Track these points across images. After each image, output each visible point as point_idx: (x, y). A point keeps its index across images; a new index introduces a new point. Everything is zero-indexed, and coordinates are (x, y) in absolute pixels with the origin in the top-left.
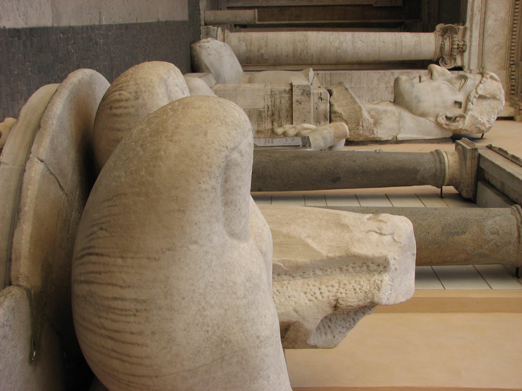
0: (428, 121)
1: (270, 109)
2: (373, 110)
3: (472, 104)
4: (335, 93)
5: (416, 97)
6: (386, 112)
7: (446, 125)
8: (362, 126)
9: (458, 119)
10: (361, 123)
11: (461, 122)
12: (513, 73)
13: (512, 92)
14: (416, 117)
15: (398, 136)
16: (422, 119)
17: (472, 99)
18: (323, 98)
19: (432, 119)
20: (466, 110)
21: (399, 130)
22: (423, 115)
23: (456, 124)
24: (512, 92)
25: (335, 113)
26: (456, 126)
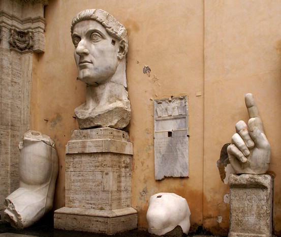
1: (117, 168)
5: (107, 69)
6: (111, 91)
9: (122, 46)
15: (126, 87)
19: (119, 62)
20: (118, 39)
23: (126, 47)
25: (116, 125)
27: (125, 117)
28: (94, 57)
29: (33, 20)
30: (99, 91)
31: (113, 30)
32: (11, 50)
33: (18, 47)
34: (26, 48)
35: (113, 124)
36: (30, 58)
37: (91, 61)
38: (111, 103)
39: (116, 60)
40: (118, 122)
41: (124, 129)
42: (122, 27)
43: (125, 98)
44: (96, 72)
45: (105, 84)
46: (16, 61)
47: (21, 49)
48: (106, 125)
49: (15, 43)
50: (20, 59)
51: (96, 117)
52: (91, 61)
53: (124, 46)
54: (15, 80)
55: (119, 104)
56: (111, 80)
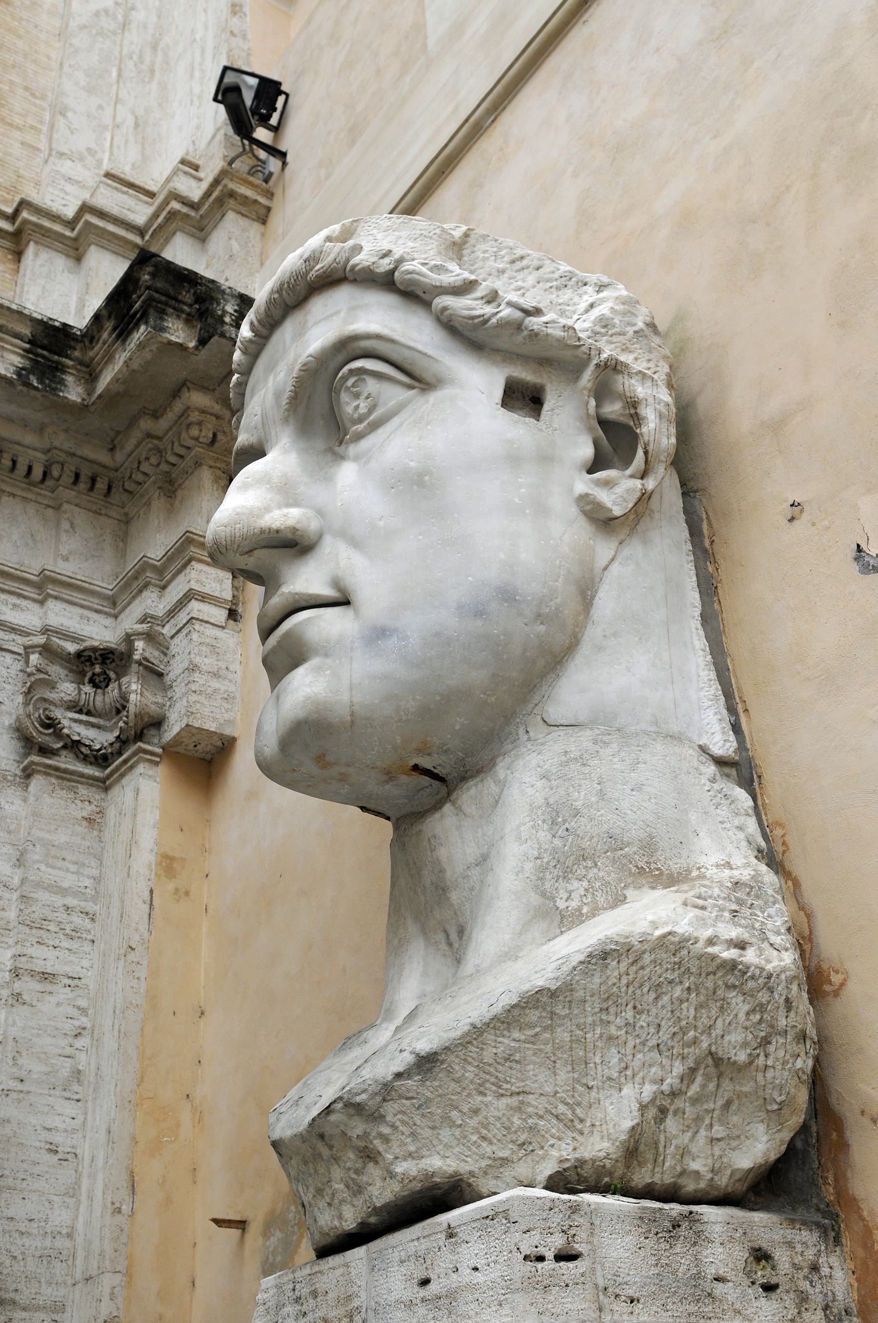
0: (615, 568)
2: (548, 897)
3: (537, 312)
4: (440, 1163)
5: (479, 613)
6: (556, 816)
7: (643, 476)
8: (742, 945)
9: (613, 410)
10: (731, 954)
11: (641, 391)
12: (22, 468)
13: (101, 485)
14: (592, 634)
15: (718, 750)
16: (606, 603)
17: (506, 312)
18: (558, 1242)
19: (604, 549)
21: (676, 738)
22: (586, 591)
24: (101, 485)
25: (632, 1151)
26: (661, 416)
27: (735, 1044)
28: (355, 543)
29: (160, 571)
30: (454, 835)
31: (492, 298)
32: (28, 774)
33: (74, 746)
34: (123, 742)
35: (598, 1147)
36: (146, 791)
37: (336, 584)
38: (568, 920)
39: (569, 532)
40: (660, 1109)
41: (766, 1188)
42: (601, 287)
43: (722, 847)
44: (378, 666)
45: (501, 770)
46: (61, 837)
47: (101, 759)
48: (522, 1170)
49: (50, 724)
50: (90, 820)
51: (387, 1090)
52: (336, 584)
53: (633, 404)
54: (45, 958)
55: (650, 913)
56: (555, 712)
